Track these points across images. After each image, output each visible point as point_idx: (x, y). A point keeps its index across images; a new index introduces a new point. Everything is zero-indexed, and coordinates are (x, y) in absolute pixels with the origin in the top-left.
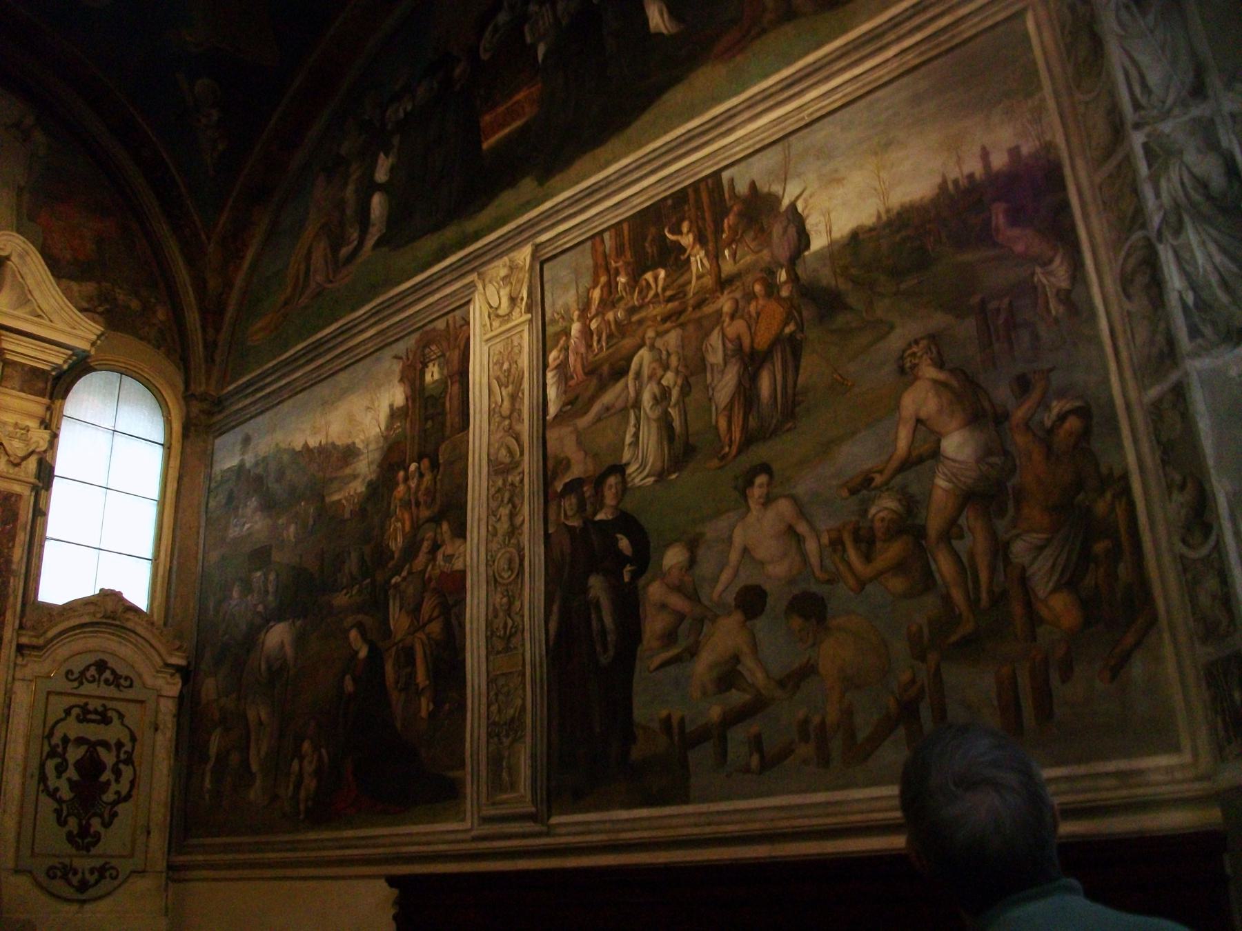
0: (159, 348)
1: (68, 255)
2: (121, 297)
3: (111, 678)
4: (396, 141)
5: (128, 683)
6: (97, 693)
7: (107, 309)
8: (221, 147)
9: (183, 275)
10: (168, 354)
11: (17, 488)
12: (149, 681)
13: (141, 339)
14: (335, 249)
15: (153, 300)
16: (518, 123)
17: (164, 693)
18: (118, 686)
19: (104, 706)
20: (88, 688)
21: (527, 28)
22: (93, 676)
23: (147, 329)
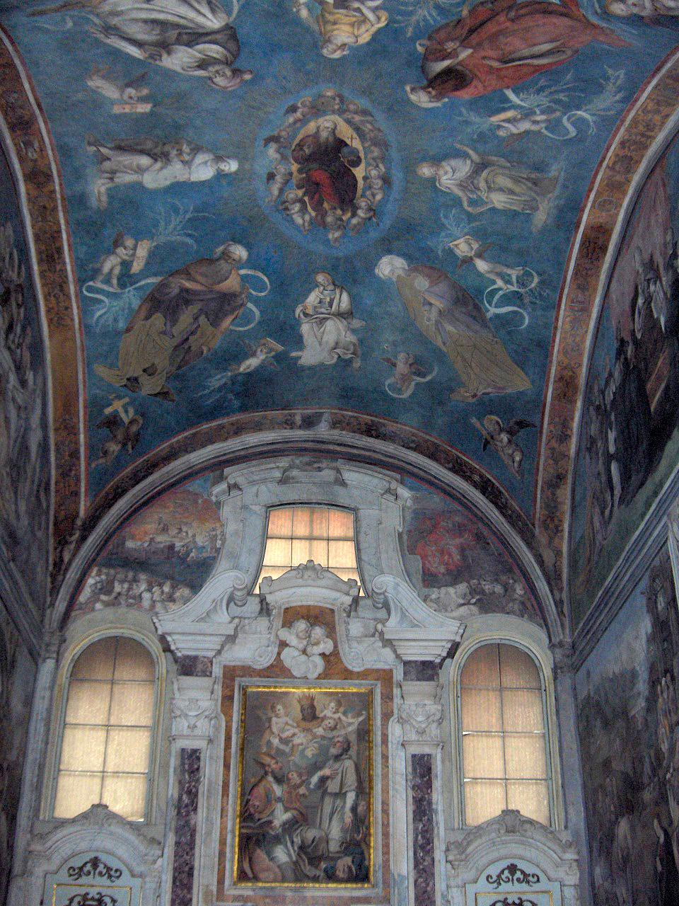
0: (523, 617)
1: (442, 569)
2: (487, 587)
3: (522, 877)
4: (613, 418)
5: (536, 879)
6: (516, 890)
7: (478, 600)
8: (517, 459)
9: (527, 557)
10: (531, 618)
11: (427, 750)
12: (552, 874)
13: (508, 613)
14: (603, 513)
15: (511, 581)
16: (663, 386)
17: (567, 883)
18: (528, 882)
19: (520, 899)
20: (504, 887)
21: (652, 304)
22: (507, 877)
23: (511, 605)
